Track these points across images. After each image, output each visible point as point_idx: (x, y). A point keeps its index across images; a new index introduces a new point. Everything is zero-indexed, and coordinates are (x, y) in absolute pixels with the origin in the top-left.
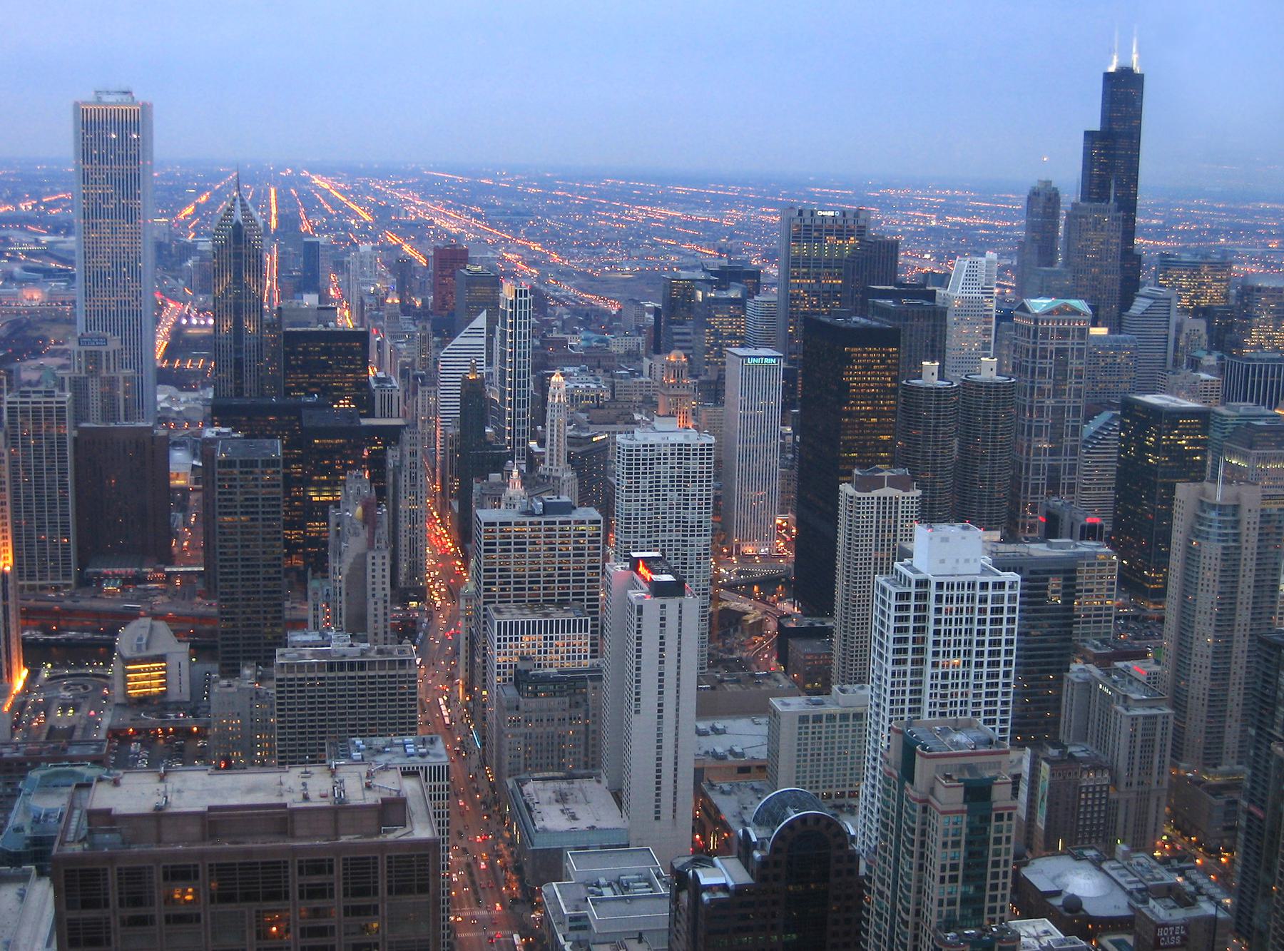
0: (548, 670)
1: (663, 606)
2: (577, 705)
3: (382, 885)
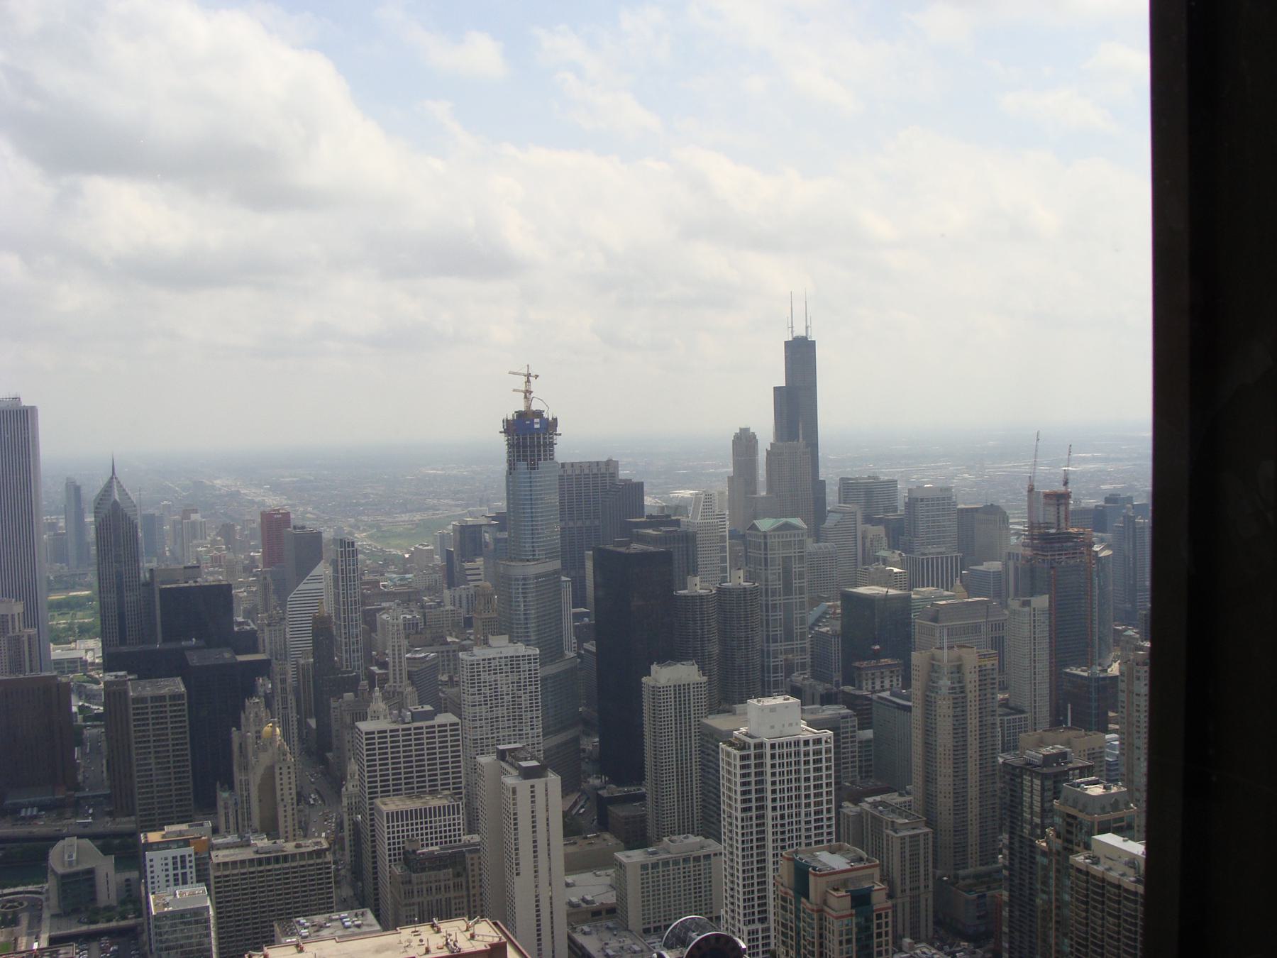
0: (431, 848)
1: (532, 786)
2: (458, 875)
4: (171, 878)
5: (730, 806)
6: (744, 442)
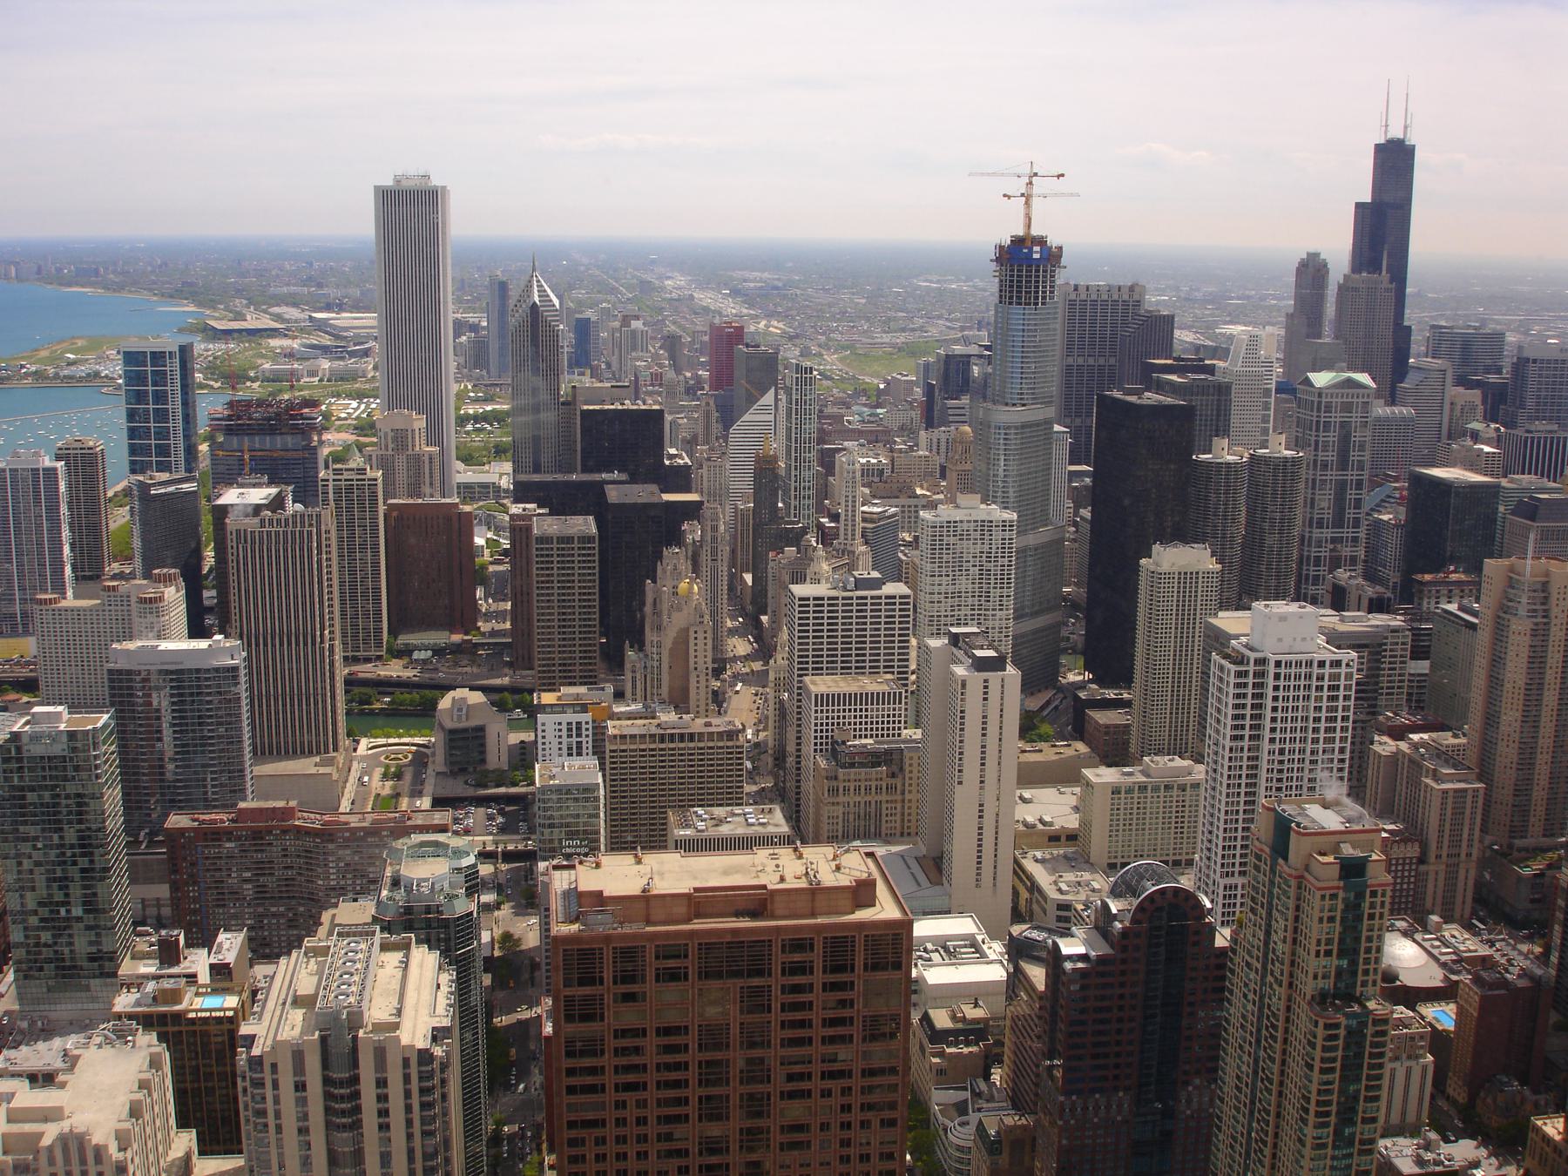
0: (864, 741)
1: (986, 681)
2: (893, 775)
3: (859, 961)
4: (564, 747)
5: (1218, 732)
6: (1312, 271)
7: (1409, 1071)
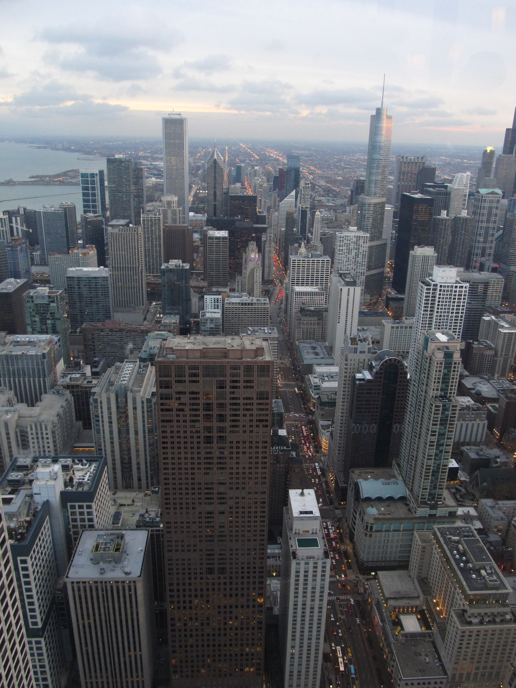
2: (320, 320)
7: (473, 425)
